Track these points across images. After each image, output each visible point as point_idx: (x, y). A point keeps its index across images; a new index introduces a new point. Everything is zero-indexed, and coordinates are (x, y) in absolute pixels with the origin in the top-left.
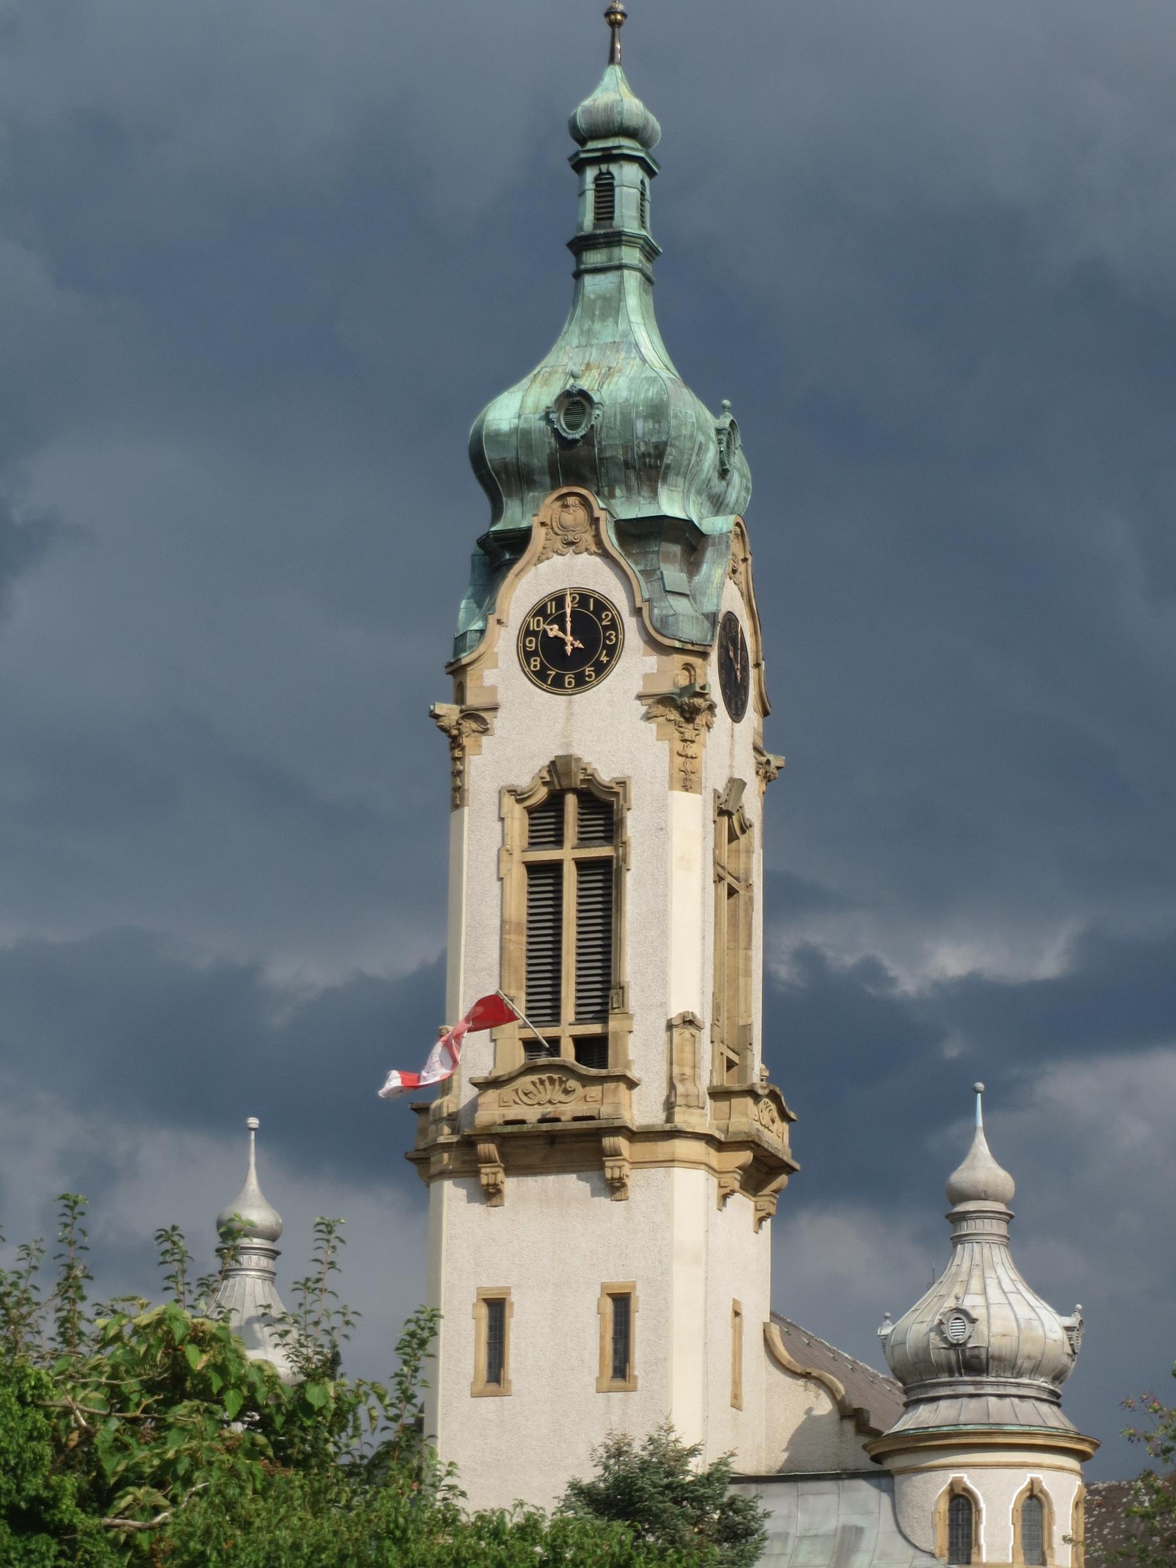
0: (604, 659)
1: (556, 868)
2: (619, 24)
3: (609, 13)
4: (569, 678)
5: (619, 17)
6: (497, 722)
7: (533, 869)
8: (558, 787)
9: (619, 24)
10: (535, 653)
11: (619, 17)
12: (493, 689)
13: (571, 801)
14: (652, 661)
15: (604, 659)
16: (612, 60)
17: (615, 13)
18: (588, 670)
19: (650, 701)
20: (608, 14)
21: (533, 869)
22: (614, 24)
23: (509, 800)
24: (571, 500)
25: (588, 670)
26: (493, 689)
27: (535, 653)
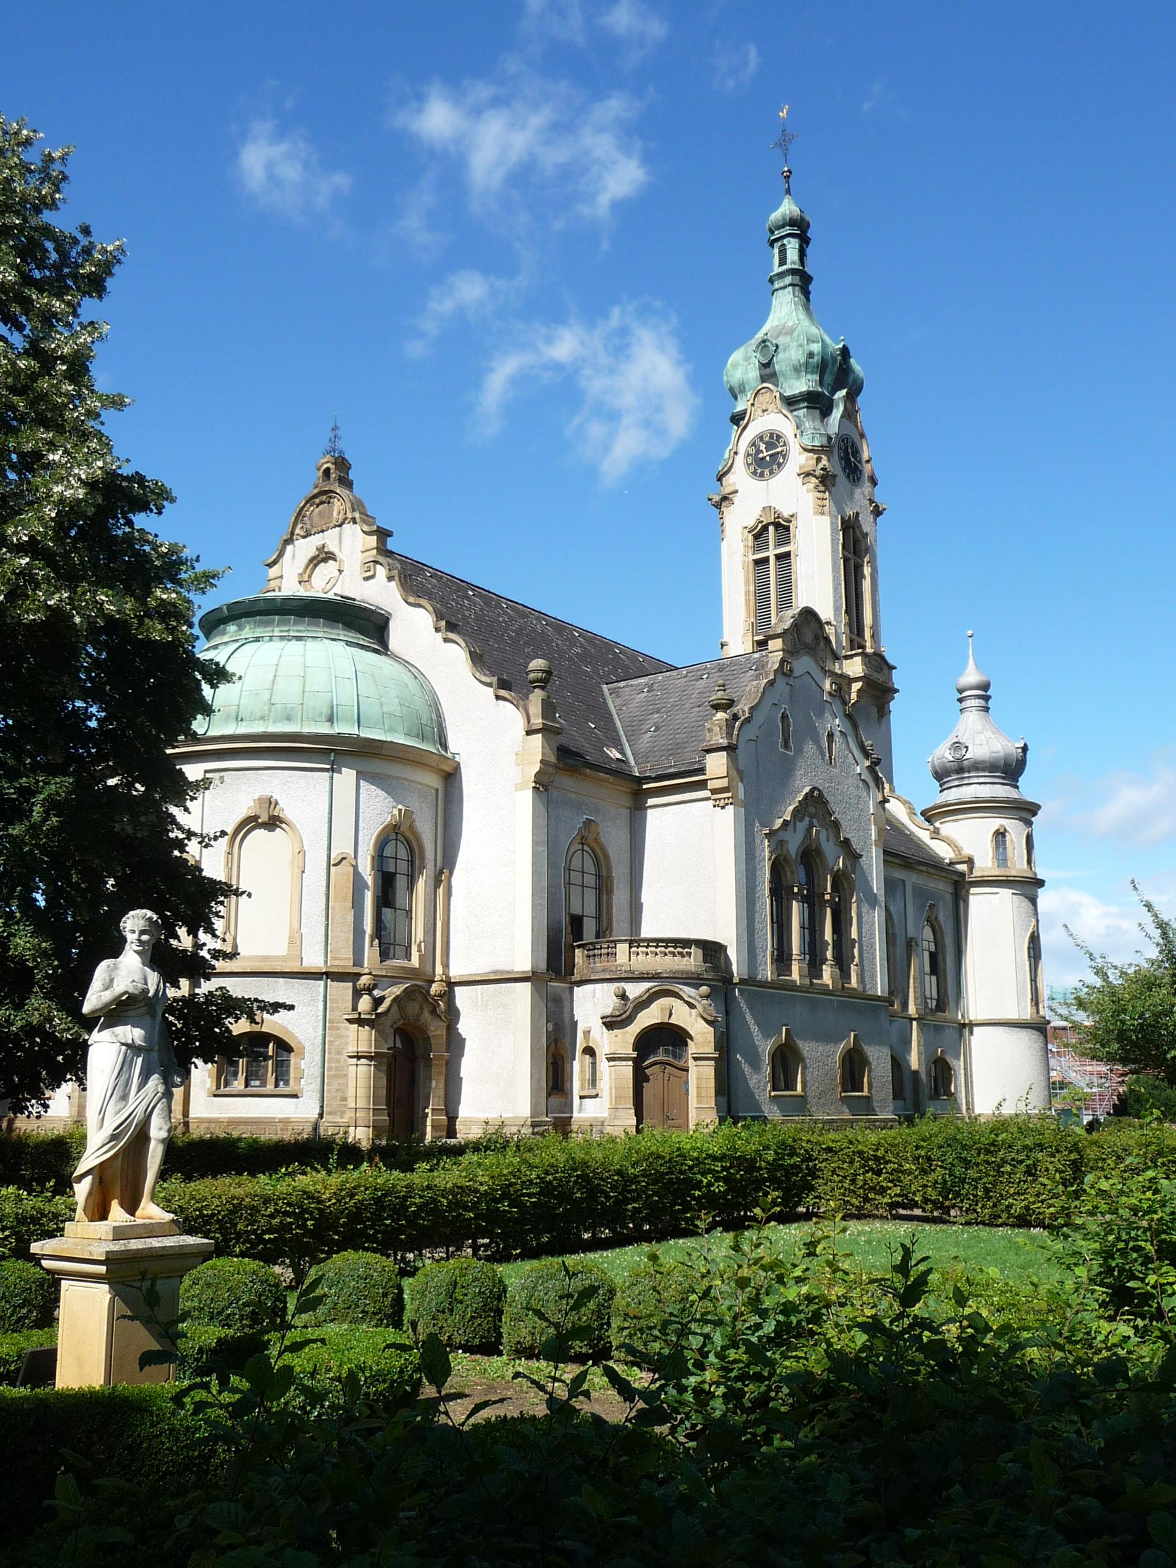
0: (781, 461)
1: (766, 560)
2: (788, 177)
4: (767, 472)
10: (752, 464)
13: (771, 528)
15: (781, 461)
18: (775, 467)
21: (757, 562)
25: (775, 467)
26: (735, 484)
27: (752, 464)
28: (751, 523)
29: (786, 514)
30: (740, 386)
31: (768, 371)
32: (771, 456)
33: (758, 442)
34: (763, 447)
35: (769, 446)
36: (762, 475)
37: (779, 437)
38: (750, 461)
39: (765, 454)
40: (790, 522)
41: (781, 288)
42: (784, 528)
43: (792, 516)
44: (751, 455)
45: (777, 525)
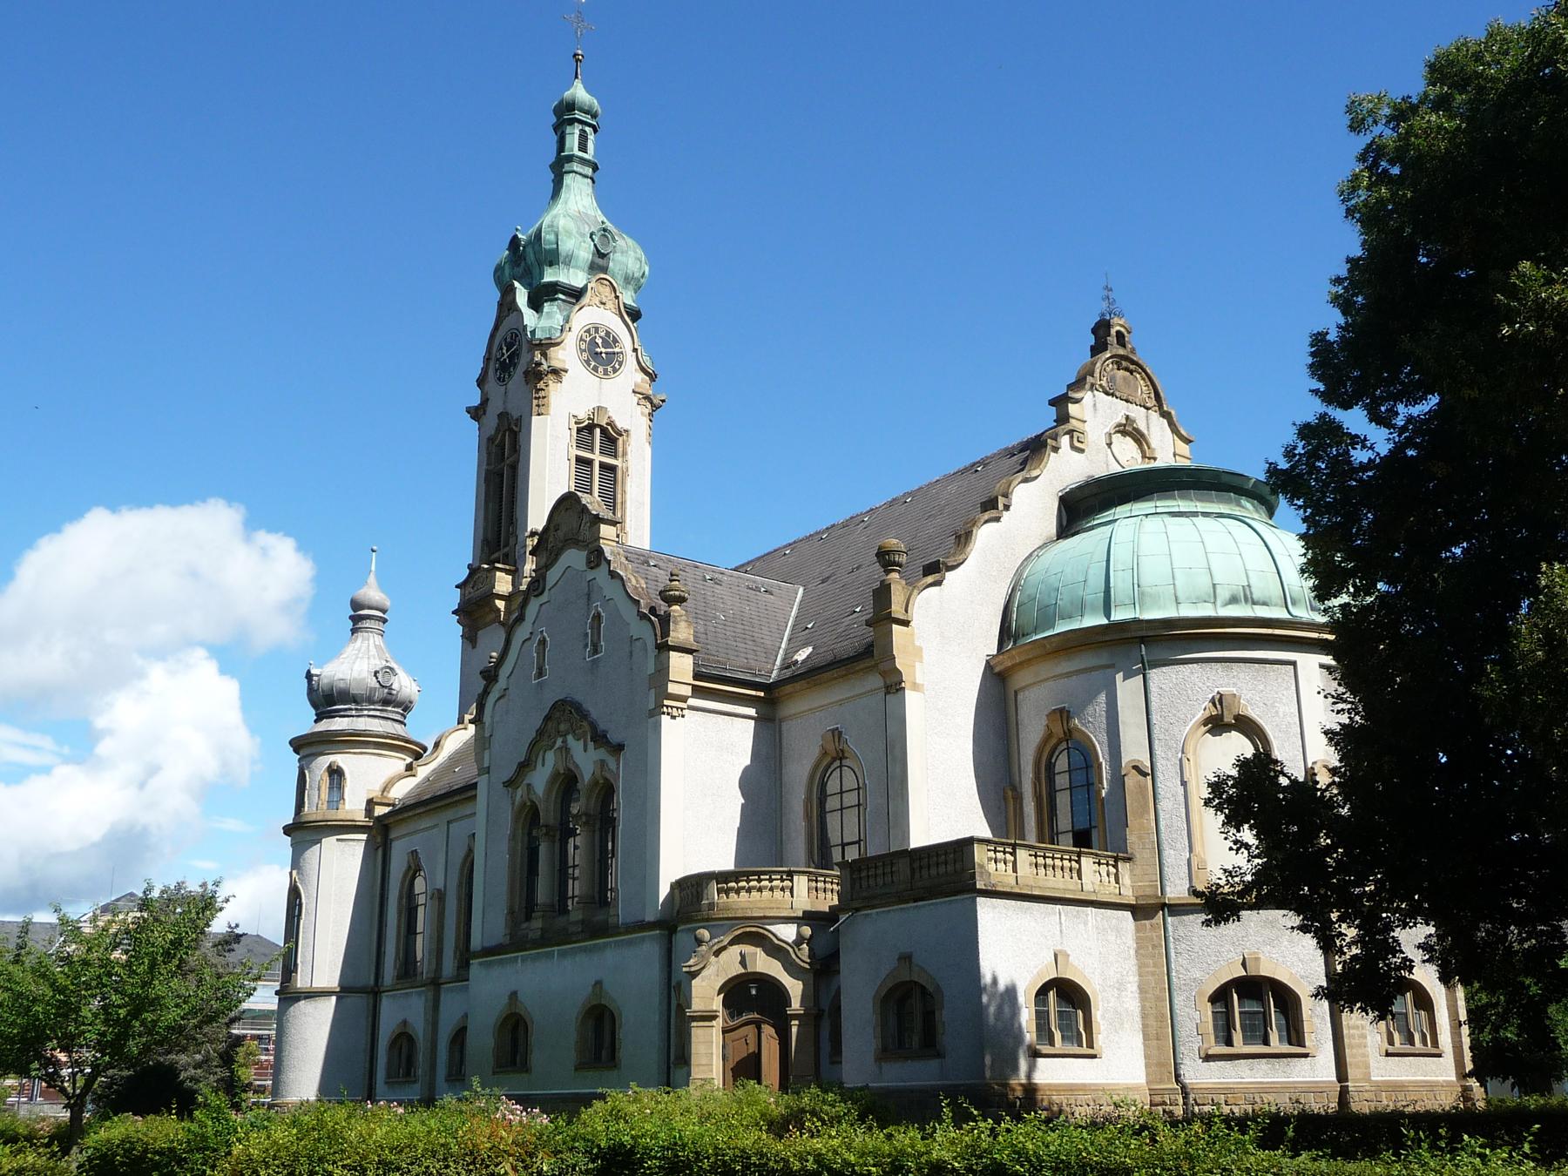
1: (589, 462)
3: (575, 55)
4: (601, 369)
5: (580, 57)
6: (566, 378)
7: (579, 460)
8: (595, 422)
9: (581, 61)
11: (580, 57)
12: (564, 361)
13: (598, 431)
14: (640, 376)
16: (576, 77)
17: (579, 55)
19: (641, 396)
20: (575, 55)
21: (579, 460)
22: (577, 60)
23: (571, 417)
24: (605, 282)
26: (564, 361)
28: (582, 415)
29: (620, 425)
30: (567, 256)
31: (600, 261)
32: (606, 353)
33: (592, 331)
34: (599, 341)
35: (606, 344)
36: (595, 369)
37: (615, 341)
38: (583, 347)
39: (603, 350)
40: (621, 435)
41: (580, 174)
42: (612, 439)
43: (626, 431)
44: (586, 342)
45: (604, 431)
